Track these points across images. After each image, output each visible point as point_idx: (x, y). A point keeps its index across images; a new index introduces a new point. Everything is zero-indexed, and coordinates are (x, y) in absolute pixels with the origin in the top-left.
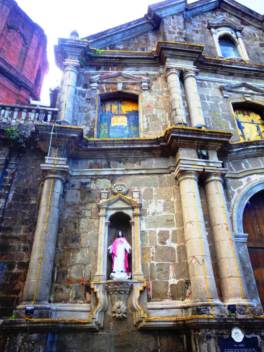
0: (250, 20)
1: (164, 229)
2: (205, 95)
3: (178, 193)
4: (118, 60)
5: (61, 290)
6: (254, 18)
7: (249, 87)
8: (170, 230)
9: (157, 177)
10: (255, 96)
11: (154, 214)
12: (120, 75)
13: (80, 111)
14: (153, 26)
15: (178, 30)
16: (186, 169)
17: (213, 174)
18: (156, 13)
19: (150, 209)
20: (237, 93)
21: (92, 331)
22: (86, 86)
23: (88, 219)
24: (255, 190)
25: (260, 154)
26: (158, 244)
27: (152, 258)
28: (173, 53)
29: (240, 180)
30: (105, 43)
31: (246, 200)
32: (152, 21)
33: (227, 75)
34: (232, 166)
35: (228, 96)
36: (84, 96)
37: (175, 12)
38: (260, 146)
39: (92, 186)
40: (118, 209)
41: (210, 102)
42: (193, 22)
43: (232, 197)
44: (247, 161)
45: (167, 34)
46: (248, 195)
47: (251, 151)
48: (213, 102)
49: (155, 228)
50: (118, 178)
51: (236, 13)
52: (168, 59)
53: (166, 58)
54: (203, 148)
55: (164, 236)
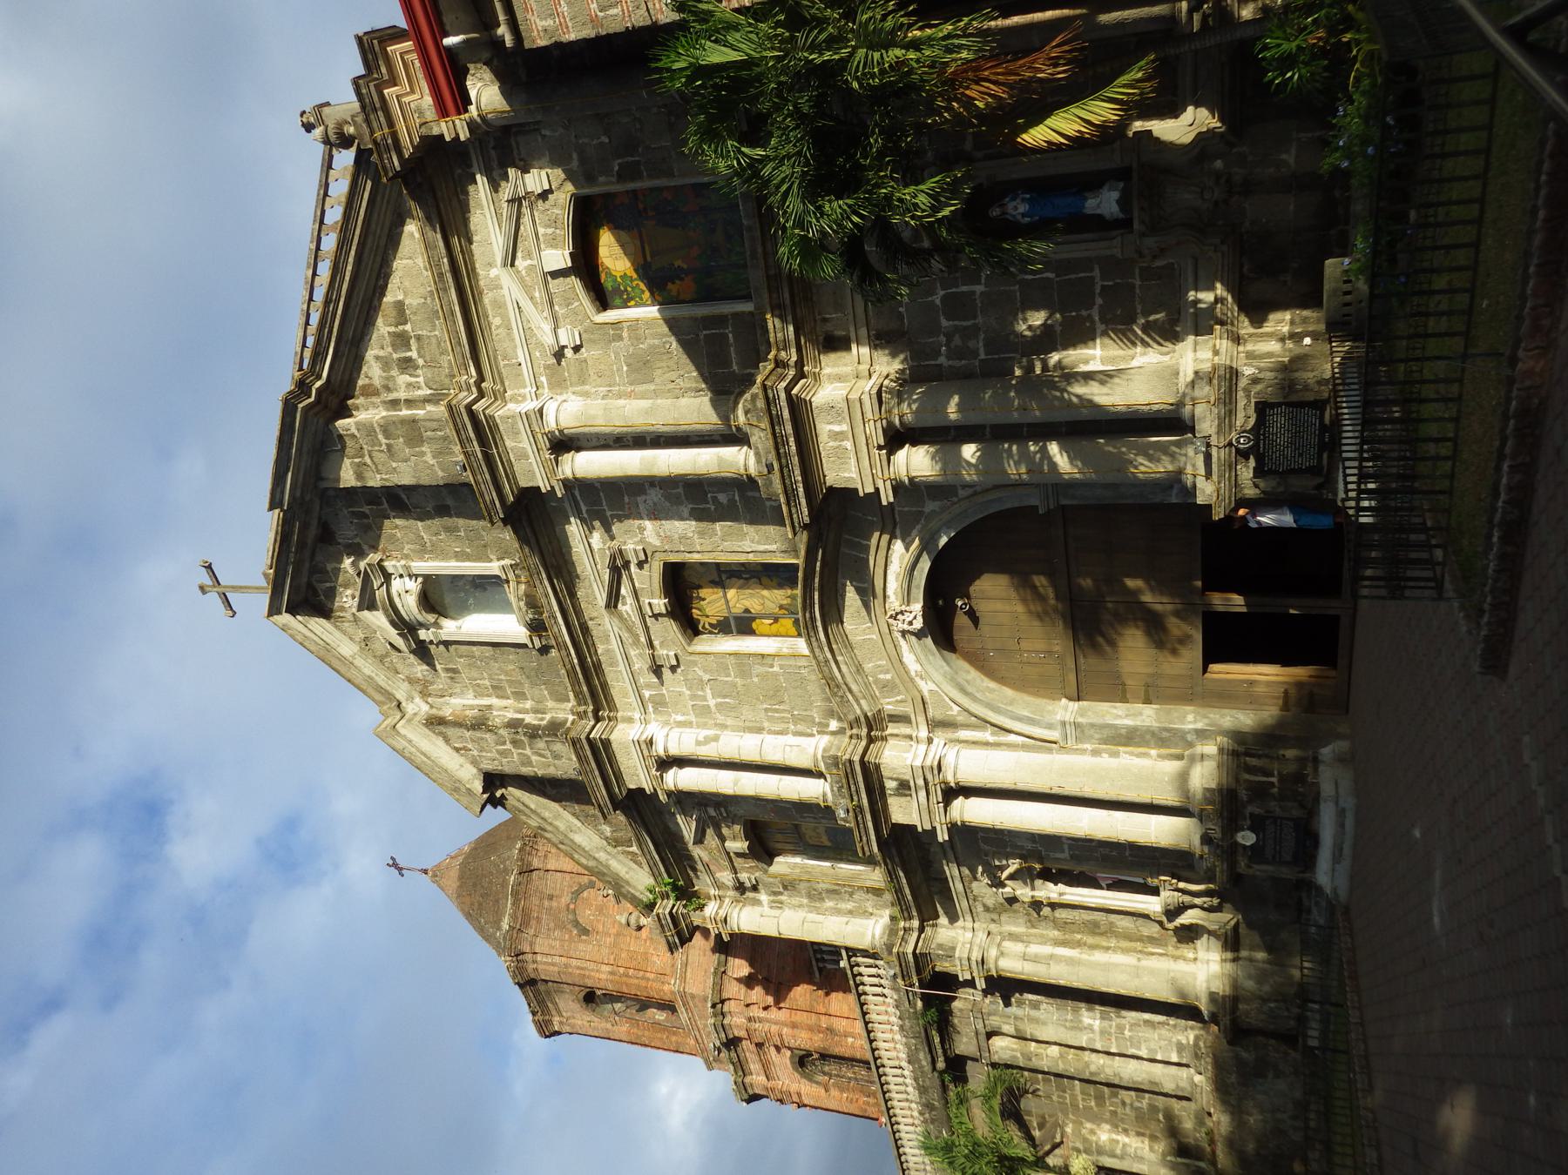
7: (613, 599)
15: (509, 746)
20: (647, 628)
29: (926, 694)
37: (440, 742)
38: (829, 656)
41: (709, 696)
47: (844, 668)
52: (632, 786)
54: (883, 788)
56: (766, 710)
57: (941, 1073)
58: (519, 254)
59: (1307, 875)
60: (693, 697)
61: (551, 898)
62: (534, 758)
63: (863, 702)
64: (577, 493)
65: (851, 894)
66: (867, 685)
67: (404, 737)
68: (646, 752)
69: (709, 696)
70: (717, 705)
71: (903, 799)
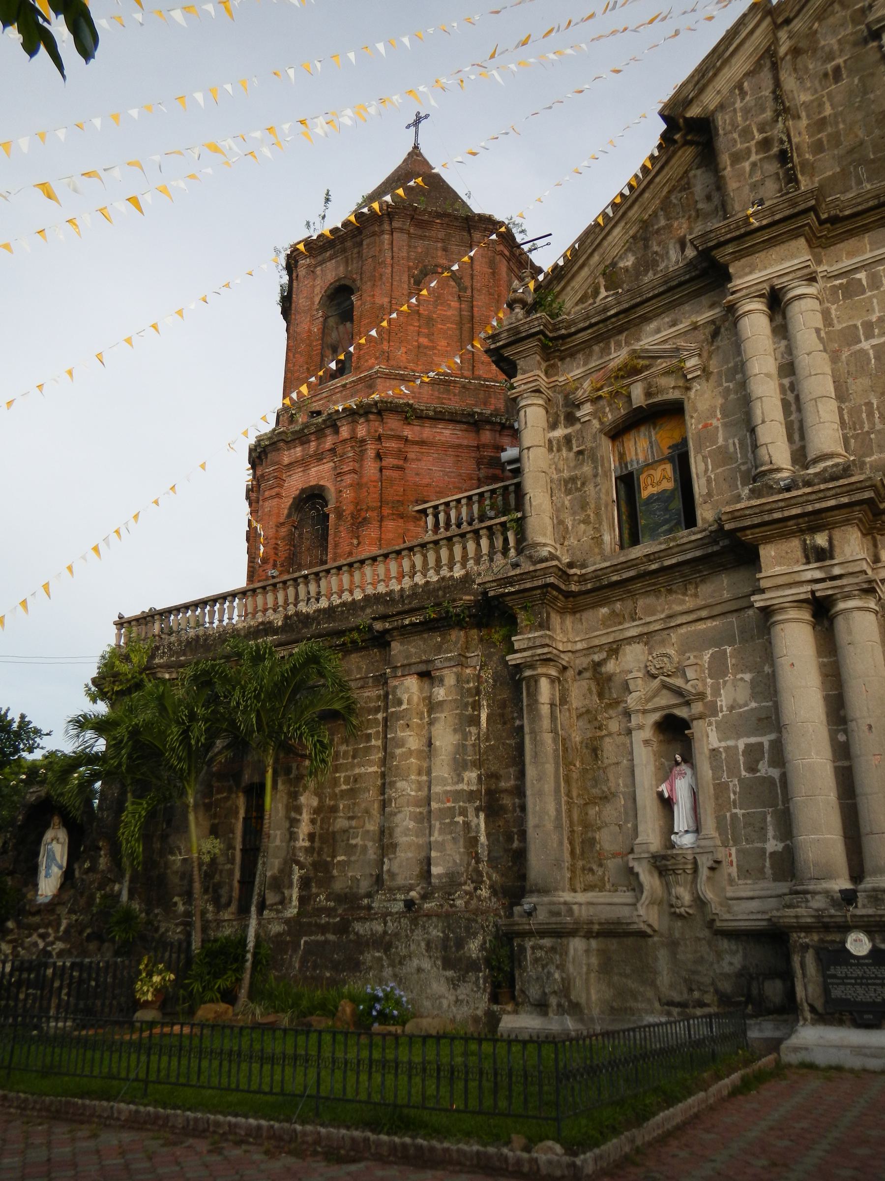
1: (753, 740)
3: (769, 654)
4: (621, 316)
5: (591, 870)
8: (765, 740)
9: (733, 619)
11: (731, 708)
12: (635, 355)
13: (568, 492)
14: (697, 144)
15: (758, 137)
16: (769, 603)
17: (839, 596)
18: (689, 115)
19: (723, 698)
21: (642, 935)
22: (571, 419)
23: (615, 736)
26: (744, 773)
27: (734, 801)
28: (739, 245)
32: (689, 138)
36: (570, 449)
37: (746, 67)
39: (611, 667)
40: (662, 708)
41: (875, 341)
42: (823, 43)
45: (729, 169)
49: (738, 738)
50: (657, 638)
52: (731, 270)
54: (814, 529)
55: (753, 753)
56: (869, 404)
57: (370, 627)
59: (808, 1015)
60: (869, 327)
61: (445, 249)
62: (747, 165)
65: (586, 521)
68: (799, 274)
69: (875, 341)
70: (862, 351)
71: (799, 554)
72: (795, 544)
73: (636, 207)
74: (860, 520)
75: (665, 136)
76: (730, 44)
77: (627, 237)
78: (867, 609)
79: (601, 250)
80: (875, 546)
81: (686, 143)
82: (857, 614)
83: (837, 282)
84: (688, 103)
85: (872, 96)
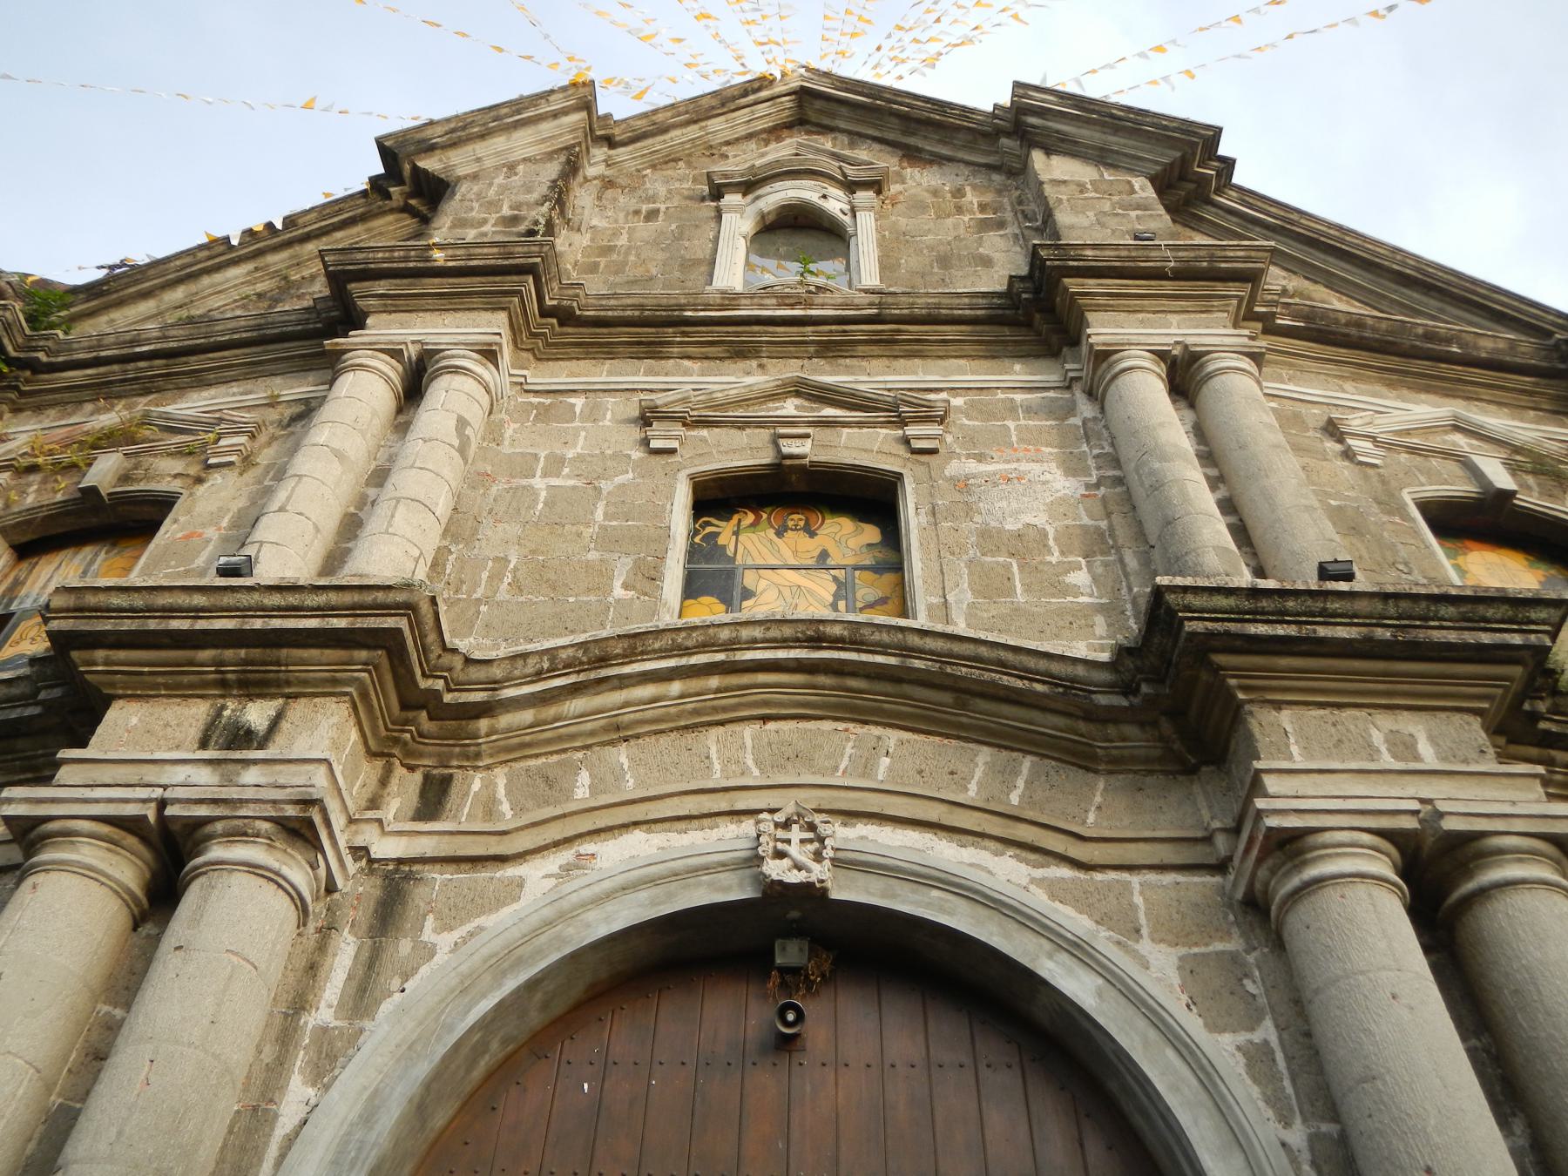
0: (941, 142)
2: (542, 455)
6: (959, 128)
10: (846, 430)
15: (506, 211)
17: (219, 827)
18: (421, 164)
24: (588, 925)
25: (715, 710)
29: (511, 871)
30: (155, 311)
31: (484, 996)
32: (413, 202)
33: (721, 359)
34: (501, 792)
35: (675, 444)
41: (555, 482)
43: (396, 983)
44: (624, 759)
46: (520, 963)
48: (571, 482)
51: (875, 126)
53: (366, 315)
54: (253, 687)
58: (1475, 442)
63: (527, 716)
64: (1051, 394)
66: (562, 742)
67: (565, 112)
69: (555, 482)
72: (197, 712)
73: (285, 254)
74: (364, 695)
75: (374, 181)
76: (519, 112)
77: (248, 290)
78: (274, 878)
79: (193, 287)
80: (384, 782)
81: (406, 209)
82: (242, 883)
83: (535, 400)
84: (430, 148)
85: (687, 244)
